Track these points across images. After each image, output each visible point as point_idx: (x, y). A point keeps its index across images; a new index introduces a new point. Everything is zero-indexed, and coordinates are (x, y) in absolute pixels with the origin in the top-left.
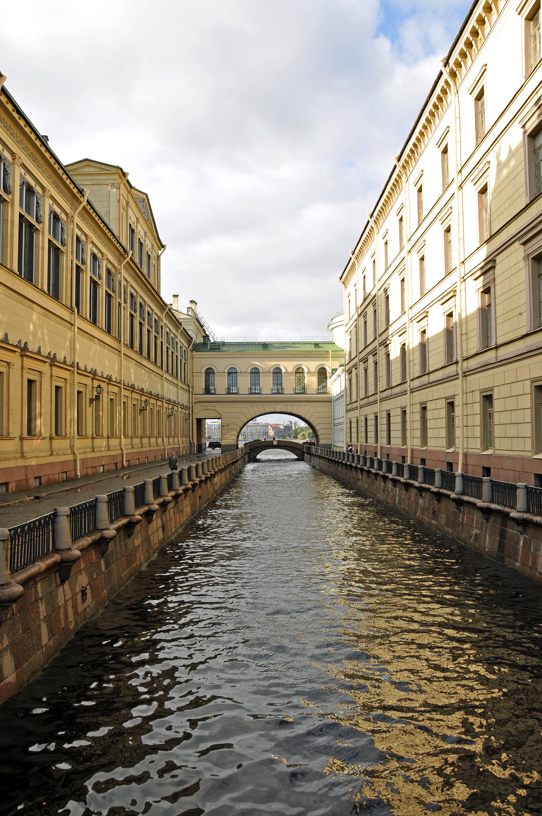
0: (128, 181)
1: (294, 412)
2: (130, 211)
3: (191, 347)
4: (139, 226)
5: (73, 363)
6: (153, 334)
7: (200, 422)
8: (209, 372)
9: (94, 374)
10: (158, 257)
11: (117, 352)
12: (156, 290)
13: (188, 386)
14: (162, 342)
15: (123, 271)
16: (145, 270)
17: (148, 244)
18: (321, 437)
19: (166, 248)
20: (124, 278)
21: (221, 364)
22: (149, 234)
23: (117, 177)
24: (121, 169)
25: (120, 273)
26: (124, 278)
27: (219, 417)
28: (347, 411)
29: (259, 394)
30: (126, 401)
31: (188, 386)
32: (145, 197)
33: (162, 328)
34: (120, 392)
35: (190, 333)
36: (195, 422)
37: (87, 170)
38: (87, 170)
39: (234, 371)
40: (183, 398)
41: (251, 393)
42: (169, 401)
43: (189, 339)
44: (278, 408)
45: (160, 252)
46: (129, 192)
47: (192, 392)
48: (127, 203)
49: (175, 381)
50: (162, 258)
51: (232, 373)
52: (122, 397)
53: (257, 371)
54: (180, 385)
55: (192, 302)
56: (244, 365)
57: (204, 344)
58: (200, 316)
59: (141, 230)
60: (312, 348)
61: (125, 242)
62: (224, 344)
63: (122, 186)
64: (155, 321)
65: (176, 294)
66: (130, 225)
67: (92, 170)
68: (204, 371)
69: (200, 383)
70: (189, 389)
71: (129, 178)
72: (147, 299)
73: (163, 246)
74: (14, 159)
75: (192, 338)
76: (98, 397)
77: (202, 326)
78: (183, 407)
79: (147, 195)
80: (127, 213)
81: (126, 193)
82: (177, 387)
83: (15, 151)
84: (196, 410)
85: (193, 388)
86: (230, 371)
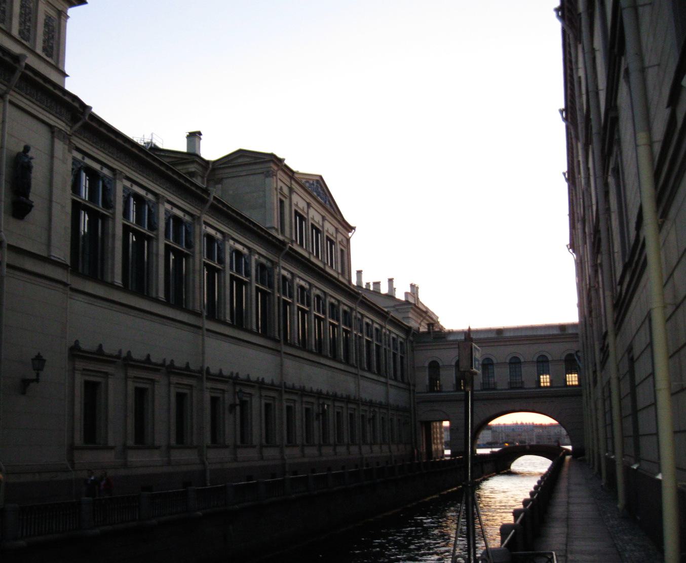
2: (295, 198)
5: (202, 368)
7: (427, 426)
8: (434, 367)
9: (235, 380)
10: (348, 240)
17: (329, 228)
22: (328, 217)
29: (494, 389)
30: (292, 405)
37: (240, 160)
38: (240, 160)
41: (512, 388)
45: (350, 234)
47: (414, 391)
49: (383, 379)
50: (351, 240)
54: (391, 382)
57: (428, 333)
59: (315, 215)
61: (288, 235)
65: (390, 277)
67: (248, 160)
68: (427, 365)
70: (409, 386)
71: (286, 162)
72: (327, 290)
73: (352, 228)
74: (115, 175)
76: (243, 404)
81: (289, 180)
83: (115, 166)
85: (414, 386)
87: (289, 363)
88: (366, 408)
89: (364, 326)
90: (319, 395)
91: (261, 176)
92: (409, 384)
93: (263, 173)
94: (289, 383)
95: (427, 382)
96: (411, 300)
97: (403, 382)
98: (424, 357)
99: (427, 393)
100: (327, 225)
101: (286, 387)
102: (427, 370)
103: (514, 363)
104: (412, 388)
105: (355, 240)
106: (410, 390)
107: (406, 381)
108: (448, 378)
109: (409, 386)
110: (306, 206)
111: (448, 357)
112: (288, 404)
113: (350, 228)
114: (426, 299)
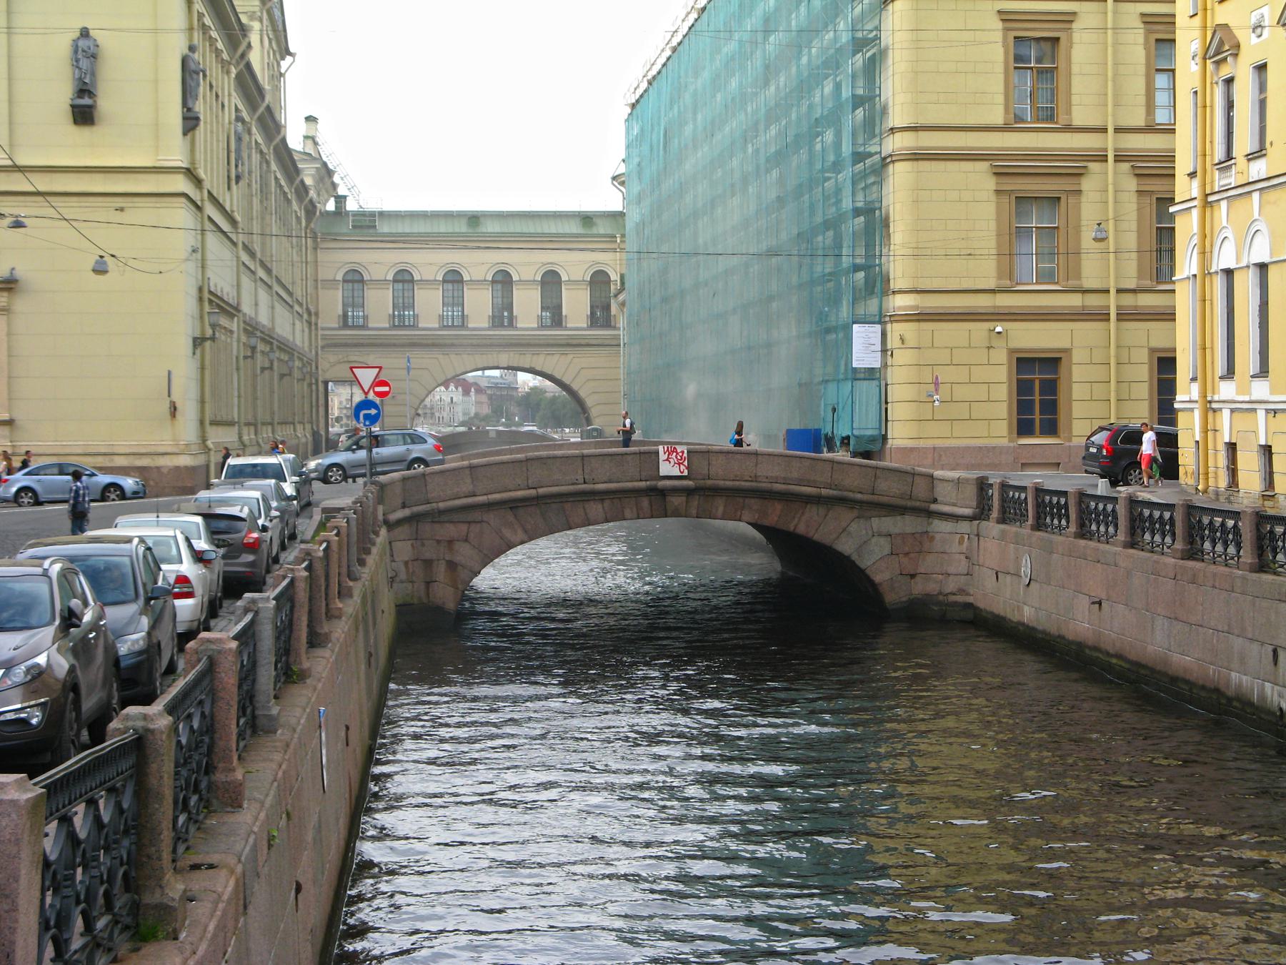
21: (379, 263)
39: (407, 277)
51: (404, 279)
56: (428, 264)
62: (381, 214)
69: (332, 304)
70: (311, 318)
84: (323, 365)
85: (317, 314)
98: (336, 262)
104: (313, 319)
108: (379, 306)
109: (311, 318)
111: (379, 263)
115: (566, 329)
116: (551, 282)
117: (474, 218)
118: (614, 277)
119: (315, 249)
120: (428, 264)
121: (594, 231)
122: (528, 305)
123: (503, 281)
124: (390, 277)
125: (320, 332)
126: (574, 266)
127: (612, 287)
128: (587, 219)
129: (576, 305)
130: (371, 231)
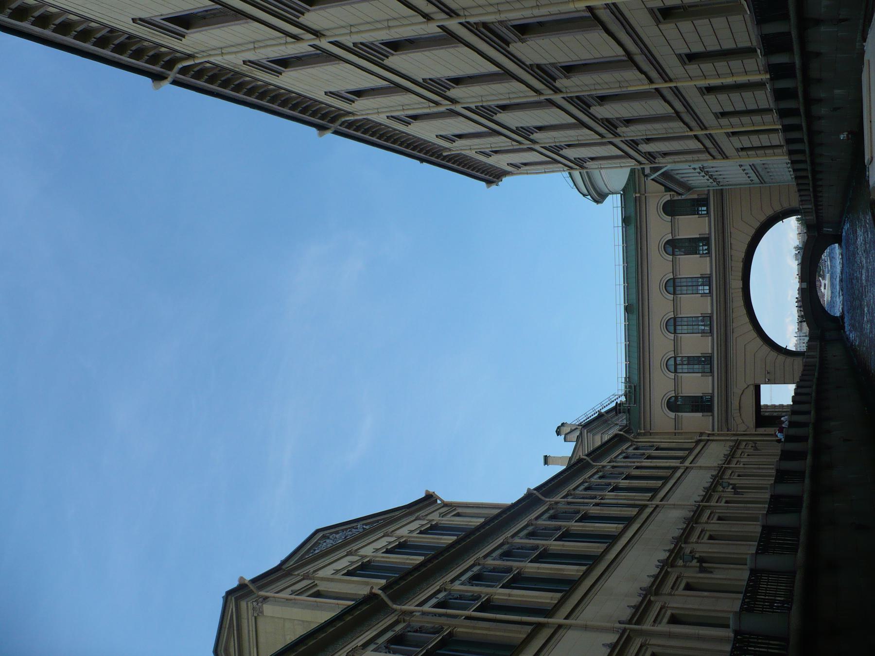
0: (254, 581)
1: (742, 255)
3: (631, 437)
4: (362, 552)
6: (575, 526)
8: (674, 405)
10: (445, 505)
11: (561, 632)
12: (496, 512)
13: (698, 442)
14: (597, 505)
15: (406, 607)
16: (449, 539)
17: (407, 530)
18: (786, 206)
19: (431, 490)
20: (421, 604)
21: (662, 386)
23: (243, 604)
24: (229, 593)
25: (411, 613)
26: (421, 604)
27: (752, 388)
28: (725, 157)
29: (711, 317)
30: (669, 613)
31: (698, 442)
32: (321, 534)
33: (569, 503)
34: (641, 633)
35: (606, 438)
36: (761, 430)
39: (672, 362)
40: (714, 455)
42: (709, 492)
43: (617, 440)
44: (736, 284)
45: (439, 502)
46: (289, 573)
47: (709, 435)
48: (306, 577)
50: (447, 498)
52: (655, 628)
53: (672, 321)
54: (687, 464)
55: (558, 433)
58: (583, 419)
60: (633, 226)
62: (628, 380)
63: (262, 593)
64: (553, 517)
66: (349, 574)
68: (672, 415)
69: (694, 421)
70: (703, 441)
72: (500, 541)
75: (616, 435)
77: (601, 415)
78: (730, 457)
79: (318, 531)
80: (322, 579)
82: (692, 468)
84: (741, 429)
85: (701, 434)
86: (672, 368)
87: (590, 613)
88: (716, 496)
89: (589, 492)
90: (666, 566)
91: (261, 621)
92: (700, 441)
93: (256, 618)
94: (627, 614)
95: (700, 414)
96: (577, 433)
97: (691, 450)
98: (661, 418)
99: (713, 416)
100: (404, 532)
101: (630, 622)
102: (680, 414)
103: (674, 287)
105: (447, 494)
106: (708, 440)
107: (692, 445)
108: (696, 384)
109: (703, 441)
110: (350, 558)
111: (662, 386)
112: (665, 620)
113: (430, 499)
114: (581, 411)
115: (710, 234)
116: (674, 246)
117: (628, 309)
118: (667, 197)
119: (651, 434)
120: (661, 345)
121: (633, 214)
122: (694, 266)
123: (673, 286)
124: (672, 375)
125: (716, 432)
126: (660, 229)
127: (676, 198)
128: (626, 221)
129: (691, 226)
130: (638, 388)
